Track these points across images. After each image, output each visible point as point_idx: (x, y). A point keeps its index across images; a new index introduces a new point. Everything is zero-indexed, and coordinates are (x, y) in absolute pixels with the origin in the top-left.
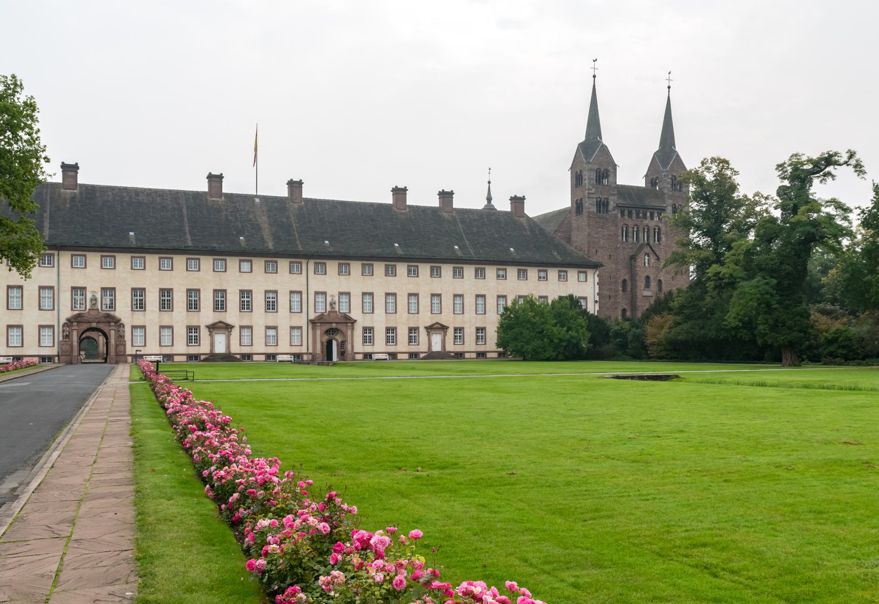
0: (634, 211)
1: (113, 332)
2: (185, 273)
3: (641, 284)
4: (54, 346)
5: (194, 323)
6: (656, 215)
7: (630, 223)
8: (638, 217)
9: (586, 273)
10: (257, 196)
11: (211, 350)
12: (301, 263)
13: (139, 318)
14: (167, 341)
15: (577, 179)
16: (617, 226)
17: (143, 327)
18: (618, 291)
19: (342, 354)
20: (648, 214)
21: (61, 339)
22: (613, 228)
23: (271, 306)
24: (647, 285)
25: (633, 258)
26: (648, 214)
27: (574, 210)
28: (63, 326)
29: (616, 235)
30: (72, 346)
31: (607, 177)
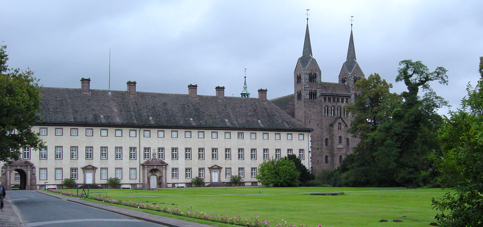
0: (332, 98)
1: (29, 172)
3: (337, 141)
5: (75, 166)
6: (345, 100)
7: (330, 105)
8: (334, 101)
9: (303, 134)
10: (109, 91)
11: (84, 182)
12: (136, 131)
13: (43, 164)
15: (298, 79)
16: (321, 106)
17: (46, 169)
18: (322, 145)
19: (160, 184)
20: (340, 100)
22: (319, 108)
23: (118, 156)
24: (340, 142)
25: (332, 125)
26: (340, 100)
27: (296, 97)
28: (2, 168)
29: (321, 112)
31: (316, 77)
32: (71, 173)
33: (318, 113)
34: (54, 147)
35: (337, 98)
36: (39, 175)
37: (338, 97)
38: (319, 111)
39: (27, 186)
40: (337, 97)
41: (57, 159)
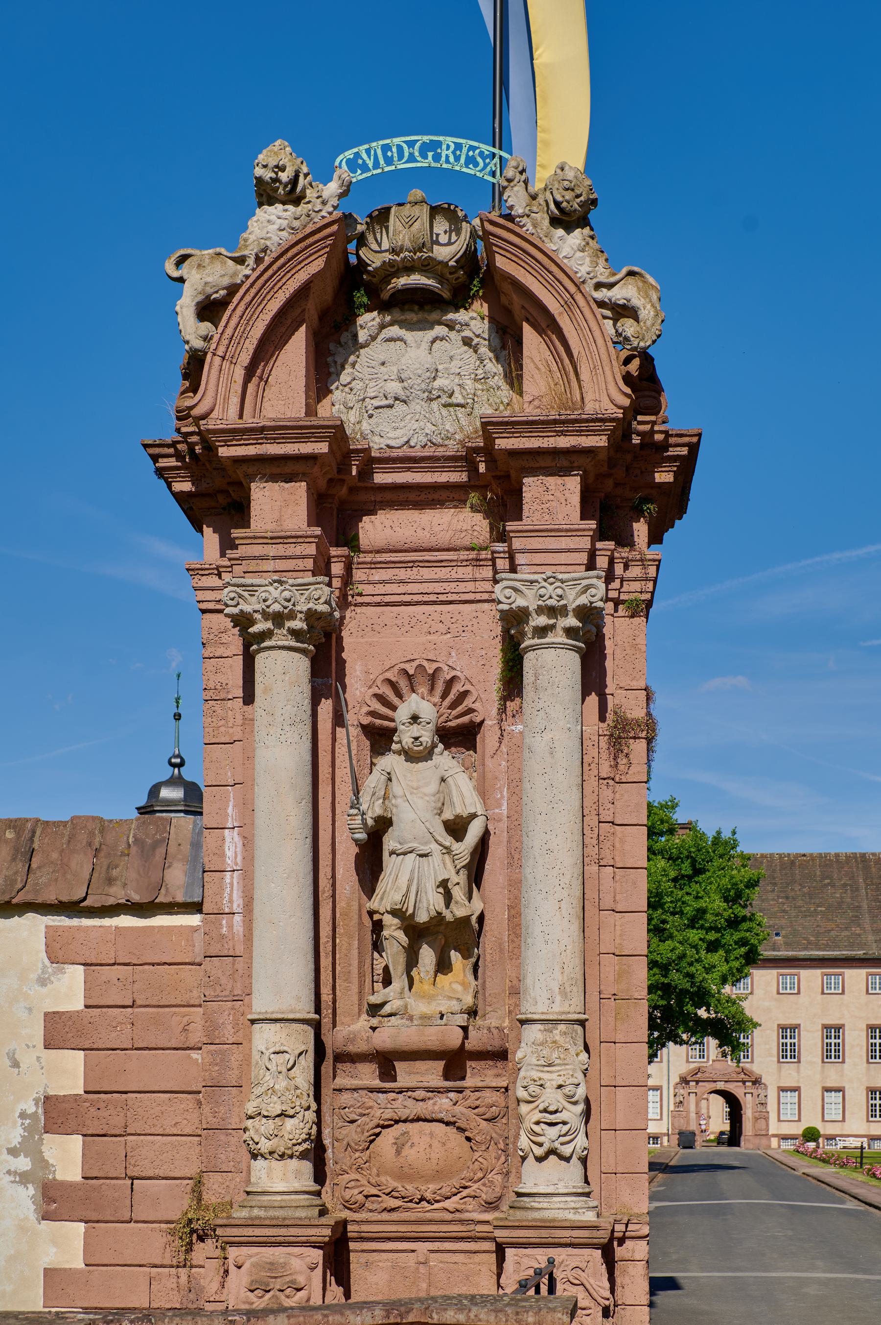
2: (864, 997)
4: (661, 1119)
13: (789, 1075)
14: (833, 1113)
21: (672, 1108)
30: (687, 1117)
32: (868, 1102)
34: (820, 1027)
36: (776, 1106)
39: (742, 1138)
41: (829, 1060)
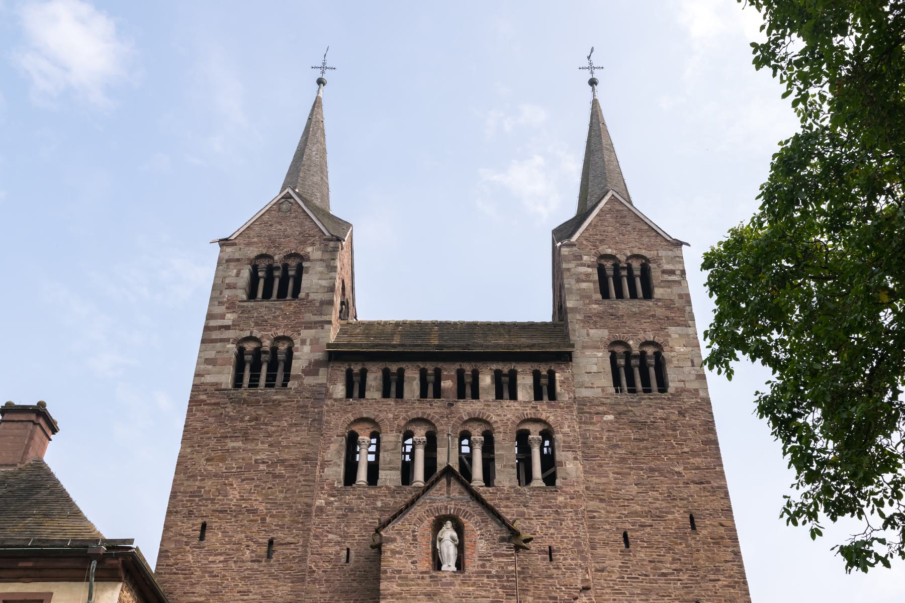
6: (525, 381)
20: (486, 380)
26: (486, 380)
33: (280, 470)
35: (460, 374)
37: (468, 368)
38: (290, 455)
40: (457, 366)
